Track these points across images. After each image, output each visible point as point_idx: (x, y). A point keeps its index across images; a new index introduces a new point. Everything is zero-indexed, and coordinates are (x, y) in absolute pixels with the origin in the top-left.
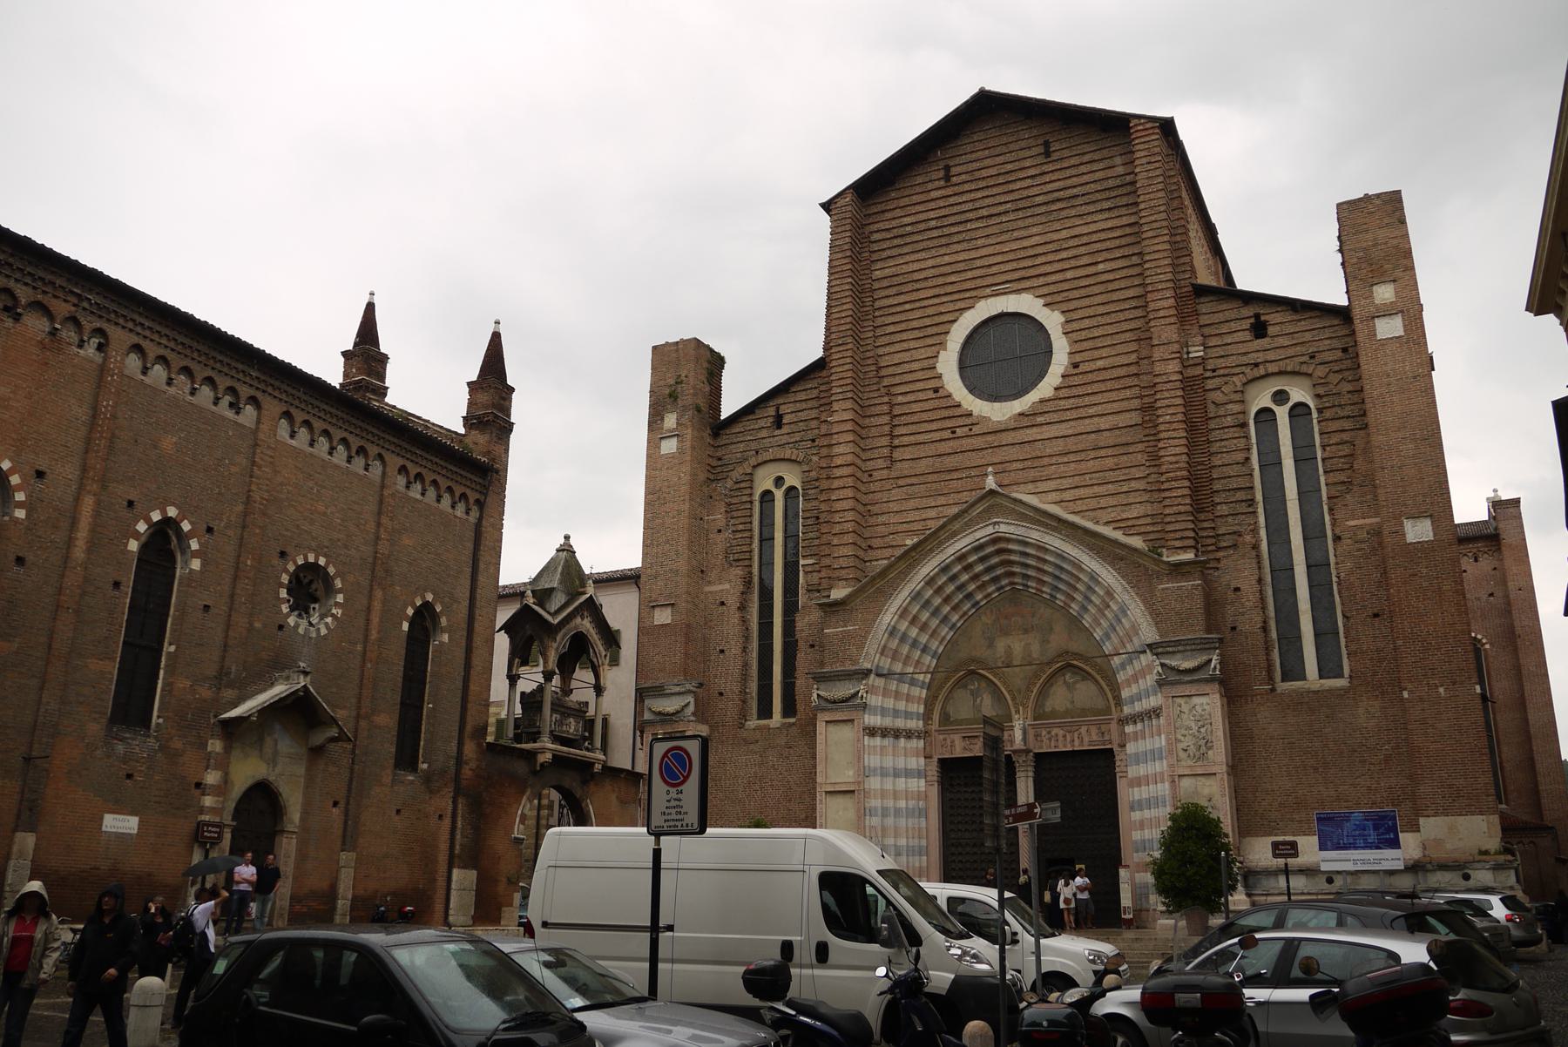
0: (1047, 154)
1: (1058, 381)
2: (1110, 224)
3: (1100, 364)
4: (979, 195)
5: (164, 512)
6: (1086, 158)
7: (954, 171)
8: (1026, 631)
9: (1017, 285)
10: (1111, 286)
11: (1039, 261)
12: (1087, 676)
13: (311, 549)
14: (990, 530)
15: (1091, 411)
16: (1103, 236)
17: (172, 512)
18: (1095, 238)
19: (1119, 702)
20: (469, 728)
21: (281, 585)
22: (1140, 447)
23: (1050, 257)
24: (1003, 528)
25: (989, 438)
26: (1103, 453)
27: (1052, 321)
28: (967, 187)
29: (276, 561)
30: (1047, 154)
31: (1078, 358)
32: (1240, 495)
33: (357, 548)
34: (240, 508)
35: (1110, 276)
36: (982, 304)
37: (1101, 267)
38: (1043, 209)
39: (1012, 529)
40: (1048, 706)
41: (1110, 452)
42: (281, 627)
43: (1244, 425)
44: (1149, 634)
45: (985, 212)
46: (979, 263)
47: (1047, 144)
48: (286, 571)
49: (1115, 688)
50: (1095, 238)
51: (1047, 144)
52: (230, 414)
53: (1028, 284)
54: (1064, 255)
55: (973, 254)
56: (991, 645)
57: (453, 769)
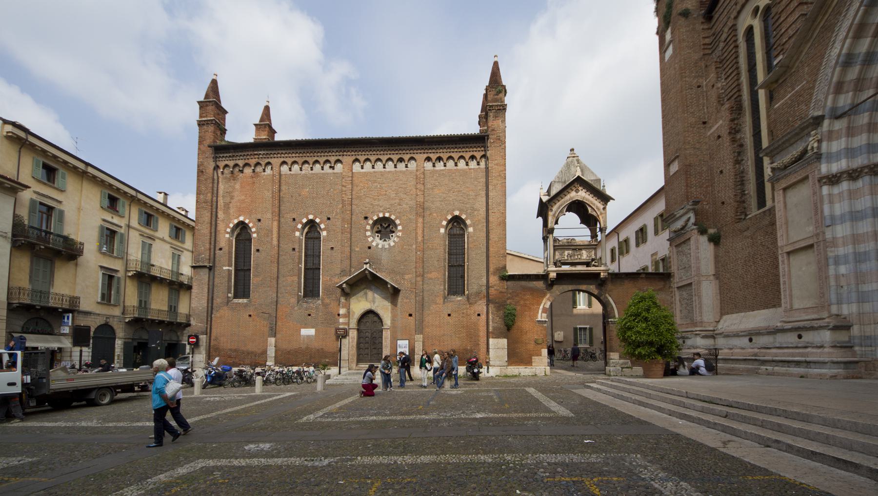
5: (307, 217)
13: (380, 212)
17: (311, 217)
20: (491, 270)
21: (367, 230)
29: (363, 222)
33: (407, 204)
34: (341, 206)
42: (369, 248)
48: (368, 224)
52: (331, 171)
57: (485, 291)
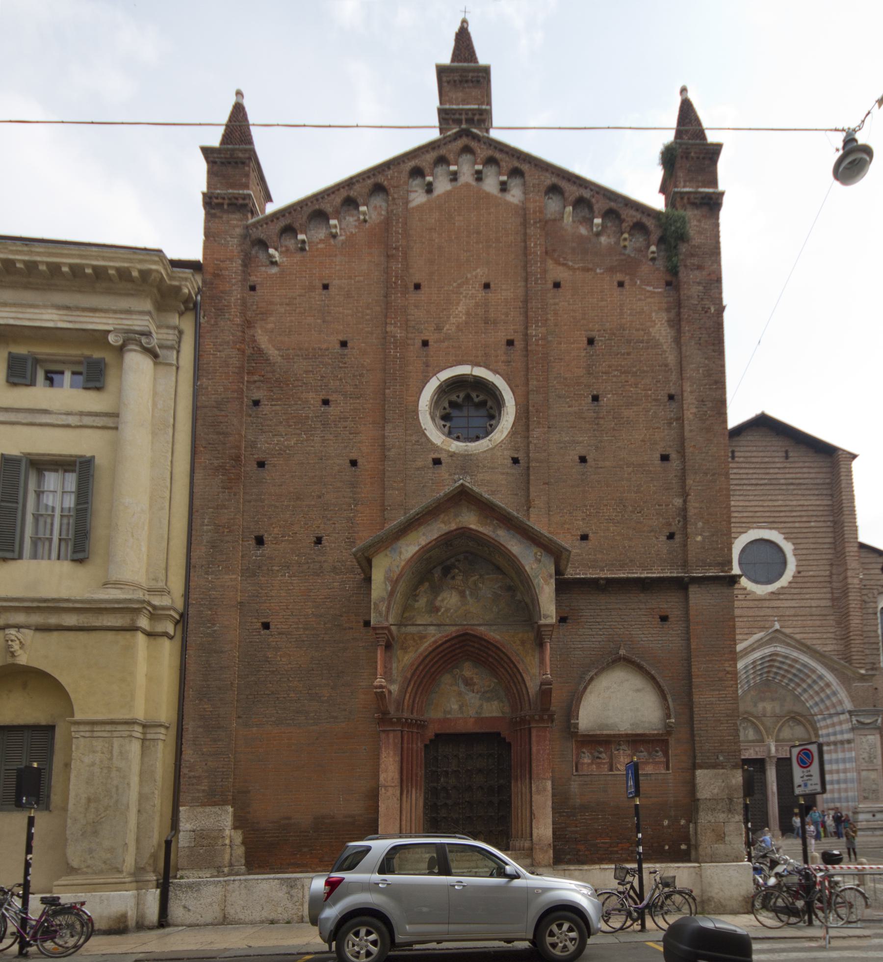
0: (787, 457)
1: (790, 579)
2: (818, 503)
3: (811, 573)
4: (751, 471)
6: (806, 464)
7: (737, 454)
8: (773, 700)
9: (771, 525)
10: (818, 535)
11: (782, 514)
12: (799, 723)
14: (772, 649)
15: (807, 596)
16: (814, 508)
18: (810, 508)
19: (817, 736)
22: (832, 617)
23: (788, 514)
24: (779, 649)
25: (756, 603)
26: (814, 618)
27: (788, 548)
28: (743, 465)
30: (787, 457)
31: (801, 569)
32: (874, 646)
35: (818, 530)
36: (751, 532)
37: (813, 524)
38: (784, 487)
39: (783, 650)
40: (781, 738)
41: (818, 618)
43: (876, 614)
44: (848, 705)
45: (753, 482)
46: (751, 509)
47: (787, 452)
49: (816, 730)
50: (810, 508)
51: (787, 452)
53: (775, 525)
54: (794, 514)
55: (747, 504)
56: (755, 706)
